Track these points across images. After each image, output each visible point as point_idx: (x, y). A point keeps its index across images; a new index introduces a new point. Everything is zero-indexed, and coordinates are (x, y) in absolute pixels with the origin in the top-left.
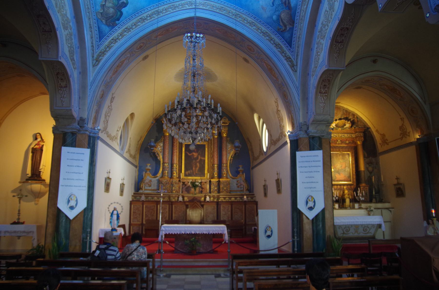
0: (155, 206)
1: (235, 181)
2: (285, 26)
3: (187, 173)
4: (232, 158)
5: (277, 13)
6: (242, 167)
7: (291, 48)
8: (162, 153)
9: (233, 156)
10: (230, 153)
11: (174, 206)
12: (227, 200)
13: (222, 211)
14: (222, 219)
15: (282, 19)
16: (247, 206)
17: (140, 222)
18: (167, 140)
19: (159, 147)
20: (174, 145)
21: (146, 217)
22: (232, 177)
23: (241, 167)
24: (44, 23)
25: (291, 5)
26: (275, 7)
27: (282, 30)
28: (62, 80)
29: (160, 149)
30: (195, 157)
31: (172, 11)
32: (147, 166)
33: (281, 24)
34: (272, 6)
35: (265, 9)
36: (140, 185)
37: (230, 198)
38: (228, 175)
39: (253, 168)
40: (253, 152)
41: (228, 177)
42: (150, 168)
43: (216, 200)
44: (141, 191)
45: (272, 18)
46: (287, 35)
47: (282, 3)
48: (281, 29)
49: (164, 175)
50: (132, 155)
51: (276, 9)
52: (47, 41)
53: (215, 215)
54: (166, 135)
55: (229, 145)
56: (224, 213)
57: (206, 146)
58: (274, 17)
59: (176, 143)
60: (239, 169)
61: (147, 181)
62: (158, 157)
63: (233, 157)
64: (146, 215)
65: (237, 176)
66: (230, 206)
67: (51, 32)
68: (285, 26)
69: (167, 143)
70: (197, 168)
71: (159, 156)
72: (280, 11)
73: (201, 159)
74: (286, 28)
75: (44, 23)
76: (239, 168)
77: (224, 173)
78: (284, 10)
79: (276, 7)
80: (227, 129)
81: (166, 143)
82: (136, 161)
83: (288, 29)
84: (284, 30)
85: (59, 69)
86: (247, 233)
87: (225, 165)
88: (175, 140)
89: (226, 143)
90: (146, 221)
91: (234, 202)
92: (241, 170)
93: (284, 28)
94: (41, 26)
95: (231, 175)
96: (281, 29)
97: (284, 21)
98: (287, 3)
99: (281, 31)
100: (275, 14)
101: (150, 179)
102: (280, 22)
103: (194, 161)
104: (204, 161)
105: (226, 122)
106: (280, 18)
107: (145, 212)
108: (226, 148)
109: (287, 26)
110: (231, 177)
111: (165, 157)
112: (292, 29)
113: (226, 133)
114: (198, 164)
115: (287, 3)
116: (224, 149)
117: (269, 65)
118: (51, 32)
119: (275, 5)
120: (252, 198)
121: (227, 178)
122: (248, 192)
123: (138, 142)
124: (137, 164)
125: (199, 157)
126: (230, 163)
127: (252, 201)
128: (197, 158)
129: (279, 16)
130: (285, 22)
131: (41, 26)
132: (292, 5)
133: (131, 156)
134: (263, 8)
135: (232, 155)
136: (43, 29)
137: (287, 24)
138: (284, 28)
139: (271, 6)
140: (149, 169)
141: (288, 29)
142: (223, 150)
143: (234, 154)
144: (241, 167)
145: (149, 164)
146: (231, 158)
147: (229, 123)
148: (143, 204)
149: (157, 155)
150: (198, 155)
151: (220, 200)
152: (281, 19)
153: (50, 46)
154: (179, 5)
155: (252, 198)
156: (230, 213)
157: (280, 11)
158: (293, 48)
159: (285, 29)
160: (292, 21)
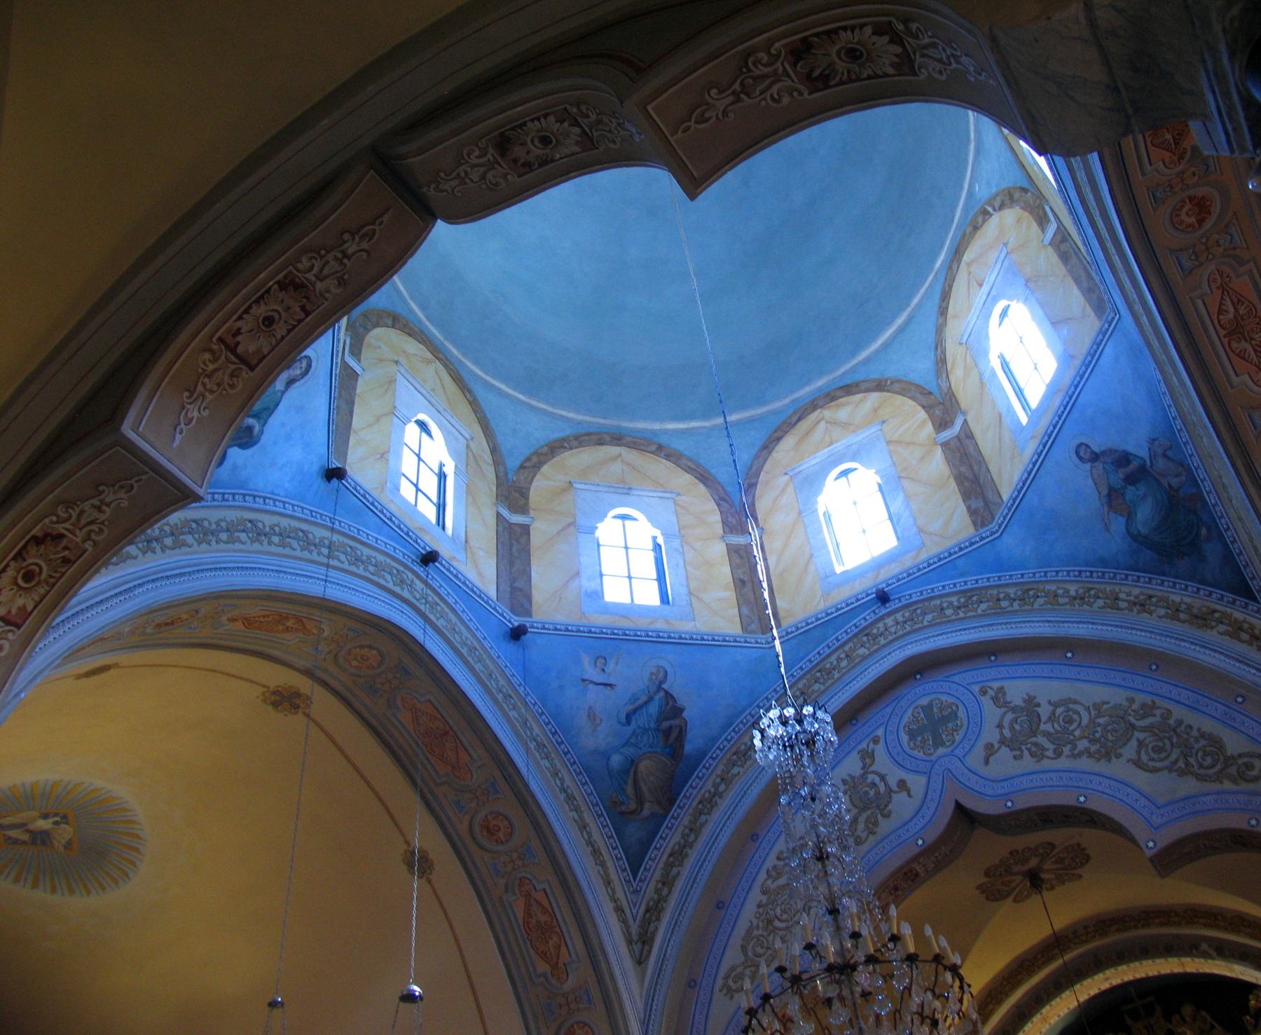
2: (640, 801)
5: (630, 751)
7: (635, 880)
15: (640, 775)
24: (269, 321)
25: (682, 746)
26: (628, 730)
27: (623, 808)
28: (29, 576)
31: (346, 566)
33: (630, 789)
34: (624, 725)
35: (598, 721)
45: (608, 759)
46: (634, 831)
47: (657, 729)
48: (622, 803)
51: (630, 738)
52: (200, 388)
58: (616, 760)
67: (252, 368)
68: (640, 801)
72: (641, 749)
74: (641, 810)
75: (269, 321)
78: (655, 752)
79: (634, 732)
83: (646, 812)
84: (631, 813)
85: (91, 523)
93: (632, 805)
94: (240, 318)
96: (622, 803)
97: (642, 785)
98: (673, 736)
99: (622, 813)
100: (622, 750)
102: (626, 783)
106: (632, 771)
109: (647, 806)
112: (658, 821)
115: (673, 736)
117: (545, 911)
118: (252, 368)
119: (633, 722)
129: (632, 763)
130: (644, 788)
131: (240, 318)
132: (688, 748)
134: (591, 715)
136: (238, 332)
137: (647, 795)
138: (632, 805)
139: (619, 722)
141: (646, 812)
152: (635, 772)
153: (196, 414)
154: (369, 558)
157: (641, 749)
158: (640, 880)
159: (636, 810)
160: (669, 794)
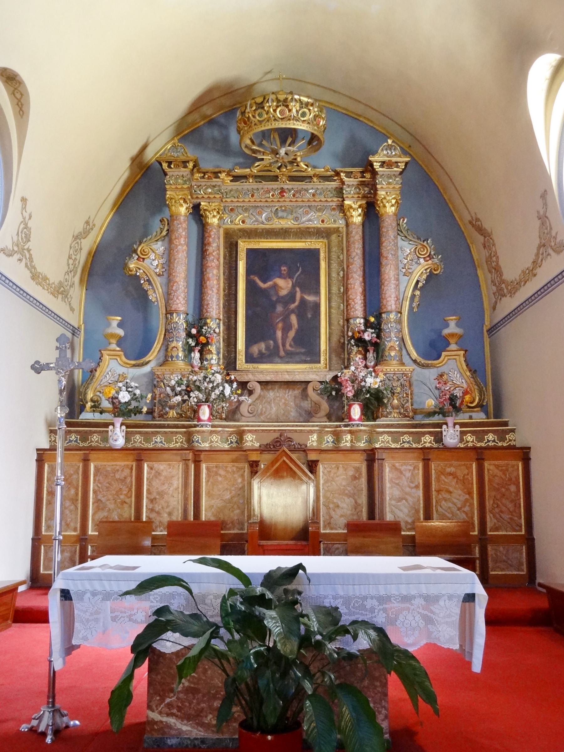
0: (132, 469)
1: (431, 374)
3: (255, 349)
4: (418, 293)
6: (457, 325)
8: (164, 279)
9: (420, 285)
10: (411, 273)
11: (204, 466)
12: (406, 445)
13: (388, 485)
14: (389, 517)
16: (486, 464)
17: (75, 530)
18: (180, 230)
19: (152, 256)
20: (206, 250)
21: (97, 510)
22: (419, 359)
23: (452, 324)
29: (155, 263)
30: (283, 293)
32: (109, 325)
36: (85, 394)
37: (418, 437)
38: (404, 352)
39: (492, 330)
40: (497, 270)
41: (406, 359)
42: (121, 332)
43: (362, 445)
44: (87, 416)
49: (172, 357)
50: (45, 279)
53: (363, 500)
54: (179, 214)
55: (406, 243)
56: (397, 493)
57: (322, 255)
59: (215, 245)
60: (446, 332)
61: (109, 378)
62: (150, 293)
63: (421, 289)
64: (97, 501)
65: (439, 357)
66: (421, 465)
69: (182, 241)
70: (292, 334)
71: (153, 288)
73: (303, 301)
76: (447, 326)
77: (388, 345)
80: (398, 186)
81: (176, 242)
82: (72, 310)
86: (492, 573)
87: (392, 316)
88: (210, 236)
89: (396, 238)
90: (99, 525)
91: (430, 448)
92: (452, 335)
95: (414, 355)
101: (121, 370)
103: (279, 308)
104: (317, 306)
105: (394, 159)
107: (95, 492)
108: (396, 256)
110: (415, 361)
111: (176, 291)
113: (394, 201)
114: (294, 319)
116: (386, 258)
120: (502, 436)
121: (403, 364)
122: (484, 417)
123: (77, 238)
124: (75, 319)
125: (298, 295)
126: (411, 308)
127: (503, 448)
128: (291, 297)
133: (35, 276)
135: (418, 282)
140: (113, 336)
142: (384, 262)
143: (424, 277)
144: (452, 324)
145: (119, 318)
146: (414, 290)
147: (406, 163)
148: (86, 461)
149: (146, 287)
150: (294, 286)
151: (377, 446)
155: (502, 436)
156: (420, 493)
